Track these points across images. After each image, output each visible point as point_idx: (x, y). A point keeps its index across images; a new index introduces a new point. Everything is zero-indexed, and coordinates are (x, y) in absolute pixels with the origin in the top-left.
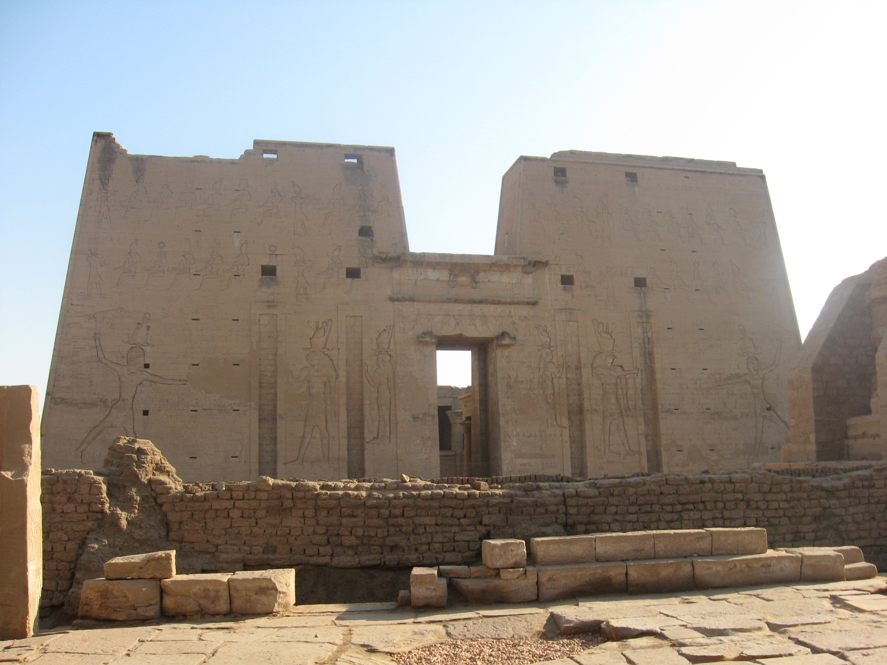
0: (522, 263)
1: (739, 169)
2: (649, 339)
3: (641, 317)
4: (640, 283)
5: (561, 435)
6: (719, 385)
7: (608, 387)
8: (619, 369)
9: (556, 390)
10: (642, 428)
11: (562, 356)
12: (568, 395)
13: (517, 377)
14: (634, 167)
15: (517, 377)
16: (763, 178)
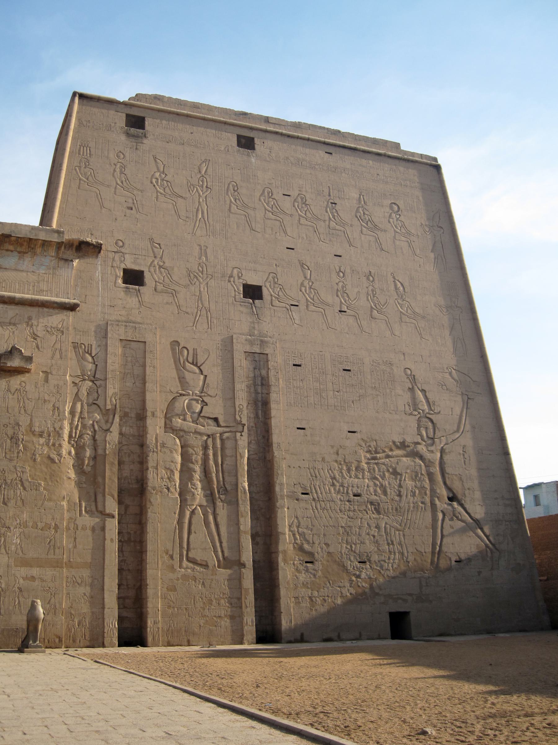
0: (55, 238)
1: (405, 152)
2: (262, 378)
3: (251, 343)
4: (253, 292)
5: (103, 529)
6: (374, 458)
7: (191, 450)
8: (210, 422)
9: (100, 451)
10: (246, 523)
11: (115, 394)
12: (120, 463)
13: (31, 425)
14: (251, 129)
15: (31, 425)
16: (438, 168)
